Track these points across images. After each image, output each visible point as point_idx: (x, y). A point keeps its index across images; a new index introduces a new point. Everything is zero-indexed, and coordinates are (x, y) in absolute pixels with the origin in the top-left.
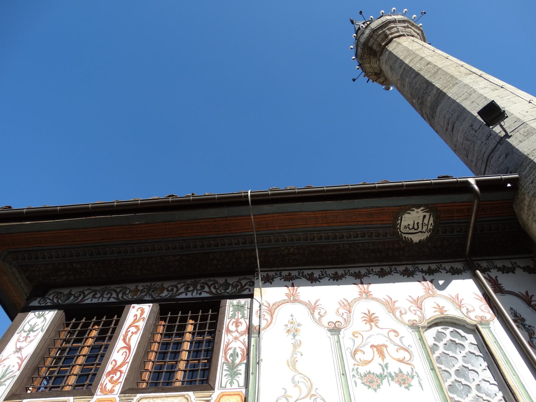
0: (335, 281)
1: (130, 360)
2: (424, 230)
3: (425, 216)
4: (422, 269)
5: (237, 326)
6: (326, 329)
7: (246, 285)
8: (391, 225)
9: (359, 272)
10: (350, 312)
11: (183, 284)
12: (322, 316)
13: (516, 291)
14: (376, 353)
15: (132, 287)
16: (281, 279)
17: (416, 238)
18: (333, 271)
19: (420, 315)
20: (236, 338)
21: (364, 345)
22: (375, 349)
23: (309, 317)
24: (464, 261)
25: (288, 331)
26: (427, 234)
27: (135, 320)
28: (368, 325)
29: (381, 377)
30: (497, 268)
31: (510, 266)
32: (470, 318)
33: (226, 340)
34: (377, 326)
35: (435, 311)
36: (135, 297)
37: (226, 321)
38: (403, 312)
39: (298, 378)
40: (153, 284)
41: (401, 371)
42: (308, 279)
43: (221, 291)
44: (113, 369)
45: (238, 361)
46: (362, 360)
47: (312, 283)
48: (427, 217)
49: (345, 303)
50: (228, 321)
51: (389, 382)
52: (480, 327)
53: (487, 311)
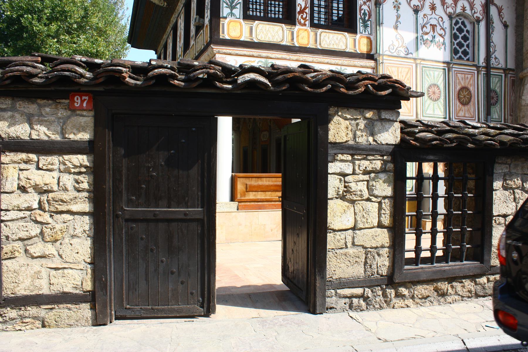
1: (308, 5)
21: (427, 24)
25: (395, 7)
45: (367, 18)
52: (476, 23)
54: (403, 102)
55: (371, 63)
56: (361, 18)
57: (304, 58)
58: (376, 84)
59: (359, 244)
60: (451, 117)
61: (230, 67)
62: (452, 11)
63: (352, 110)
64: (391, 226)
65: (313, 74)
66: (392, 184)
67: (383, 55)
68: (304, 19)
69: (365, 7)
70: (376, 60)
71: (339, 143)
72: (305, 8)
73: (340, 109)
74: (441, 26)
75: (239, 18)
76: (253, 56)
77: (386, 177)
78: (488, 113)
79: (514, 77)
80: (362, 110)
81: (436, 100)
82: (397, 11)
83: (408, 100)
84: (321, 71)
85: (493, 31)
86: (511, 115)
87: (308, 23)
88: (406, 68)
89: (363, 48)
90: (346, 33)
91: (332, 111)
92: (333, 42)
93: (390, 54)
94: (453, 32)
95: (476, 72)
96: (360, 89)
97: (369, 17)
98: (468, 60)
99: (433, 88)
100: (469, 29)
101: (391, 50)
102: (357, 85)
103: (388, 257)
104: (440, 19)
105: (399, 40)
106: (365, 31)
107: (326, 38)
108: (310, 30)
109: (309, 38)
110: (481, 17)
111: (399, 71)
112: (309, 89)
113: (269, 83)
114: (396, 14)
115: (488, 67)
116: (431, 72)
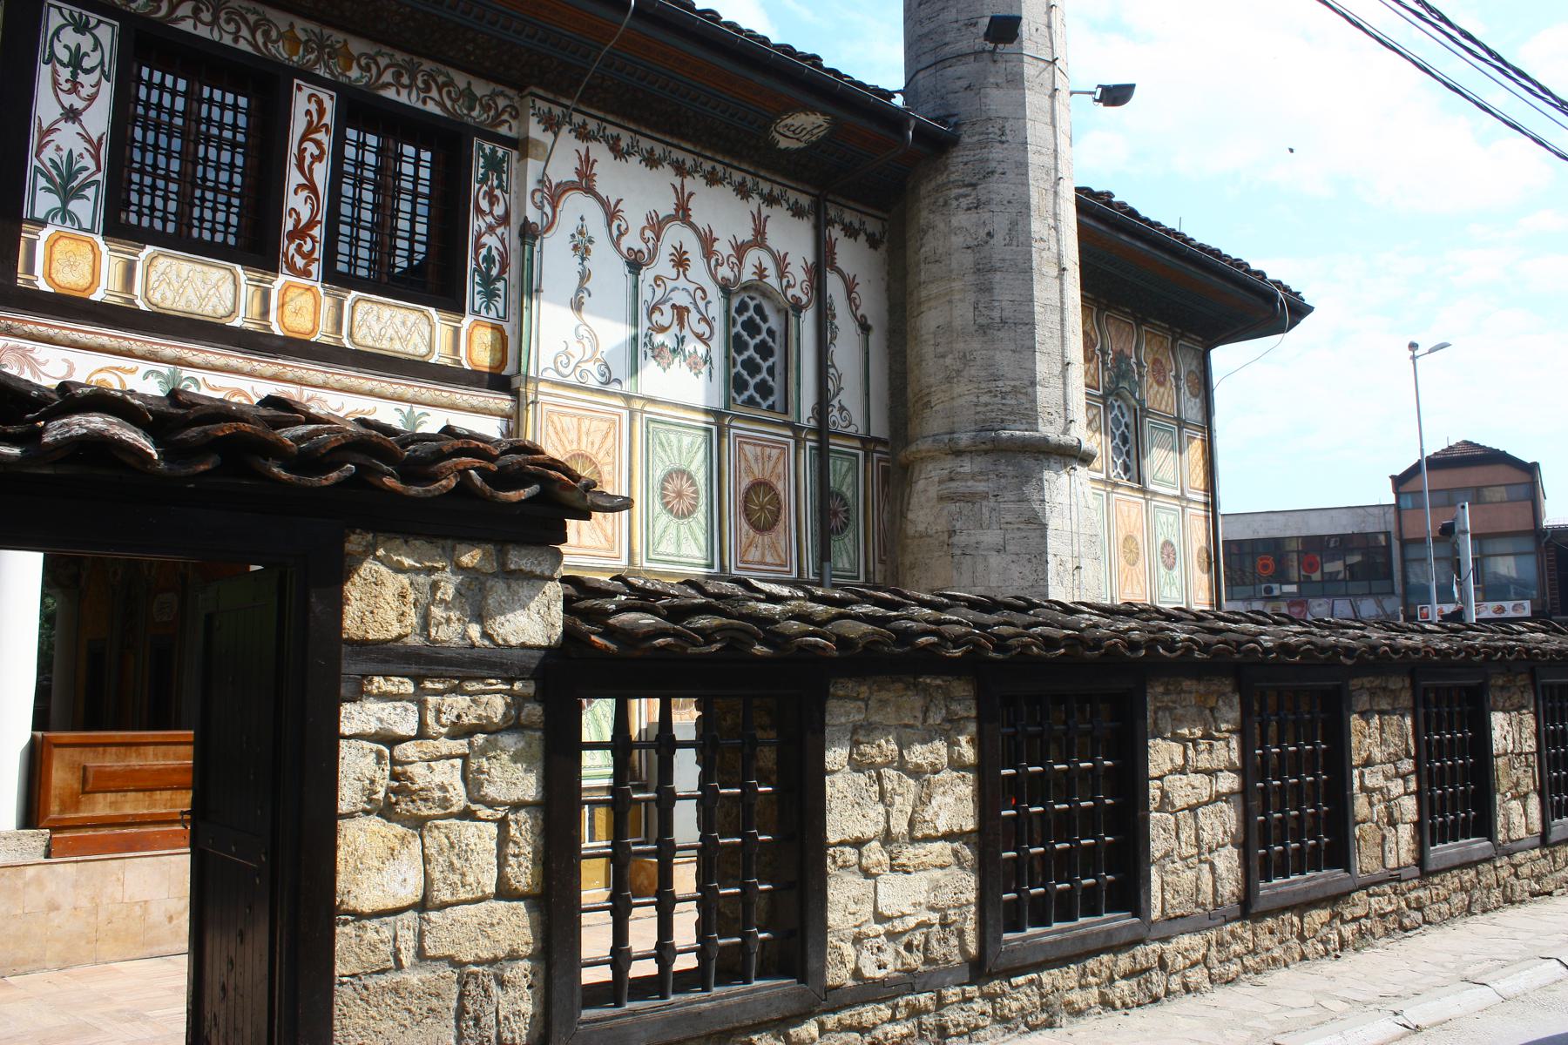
1: (322, 216)
5: (491, 204)
7: (504, 111)
12: (621, 234)
15: (281, 20)
17: (783, 143)
20: (491, 229)
21: (664, 303)
23: (605, 230)
25: (575, 248)
26: (802, 145)
27: (310, 123)
31: (857, 225)
36: (295, 58)
39: (582, 330)
40: (327, 31)
44: (295, 226)
45: (494, 272)
54: (572, 525)
55: (504, 402)
56: (477, 270)
57: (299, 373)
58: (493, 467)
59: (440, 952)
61: (22, 386)
62: (730, 275)
63: (418, 543)
64: (537, 891)
65: (301, 430)
66: (540, 764)
67: (537, 380)
68: (304, 256)
69: (490, 240)
70: (515, 394)
71: (377, 642)
72: (312, 223)
73: (381, 538)
75: (91, 231)
76: (129, 354)
77: (521, 745)
78: (824, 554)
79: (886, 461)
80: (449, 543)
81: (684, 516)
82: (583, 259)
83: (588, 518)
84: (329, 422)
85: (834, 338)
86: (882, 562)
87: (314, 268)
90: (432, 310)
91: (355, 543)
92: (390, 332)
93: (558, 378)
94: (734, 331)
95: (792, 442)
96: (444, 482)
97: (503, 270)
98: (771, 408)
99: (677, 482)
100: (774, 327)
102: (435, 468)
103: (529, 987)
104: (699, 293)
105: (585, 341)
106: (488, 308)
107: (372, 318)
108: (321, 291)
109: (316, 312)
110: (804, 299)
111: (584, 429)
112: (284, 475)
113: (153, 451)
115: (823, 431)
116: (672, 437)
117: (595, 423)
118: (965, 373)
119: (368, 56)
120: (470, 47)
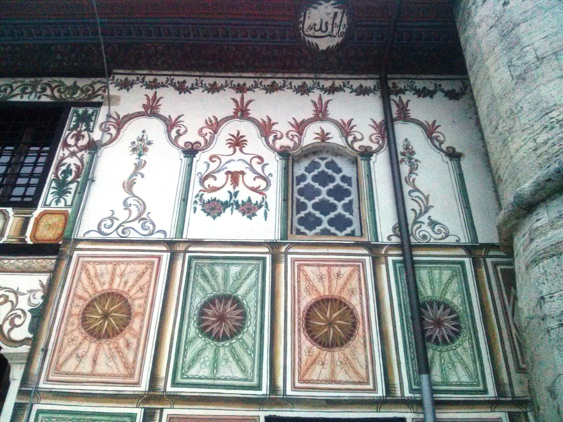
0: (210, 93)
2: (335, 33)
3: (336, 14)
4: (323, 86)
6: (180, 150)
7: (99, 90)
8: (292, 24)
9: (244, 84)
10: (215, 132)
11: (19, 84)
12: (179, 135)
13: (422, 120)
14: (230, 179)
16: (142, 86)
17: (323, 44)
18: (211, 81)
19: (297, 141)
20: (73, 154)
21: (219, 171)
22: (230, 176)
23: (164, 136)
24: (376, 79)
25: (134, 150)
26: (338, 40)
28: (232, 150)
29: (226, 205)
30: (415, 90)
31: (432, 88)
32: (353, 148)
33: (61, 155)
34: (241, 151)
35: (316, 138)
37: (66, 132)
38: (279, 136)
39: (131, 201)
41: (249, 200)
42: (177, 89)
43: (67, 96)
45: (70, 179)
46: (211, 186)
47: (180, 93)
48: (339, 16)
49: (214, 121)
50: (68, 132)
51: (232, 210)
52: (359, 158)
53: (376, 141)
60: (280, 383)
62: (291, 144)
74: (254, 171)
78: (423, 366)
82: (140, 155)
85: (413, 168)
88: (139, 263)
89: (48, 234)
93: (97, 236)
95: (368, 260)
101: (103, 229)
104: (257, 160)
114: (136, 161)
117: (129, 268)
118: (517, 126)
119: (7, 85)
120: (59, 57)
